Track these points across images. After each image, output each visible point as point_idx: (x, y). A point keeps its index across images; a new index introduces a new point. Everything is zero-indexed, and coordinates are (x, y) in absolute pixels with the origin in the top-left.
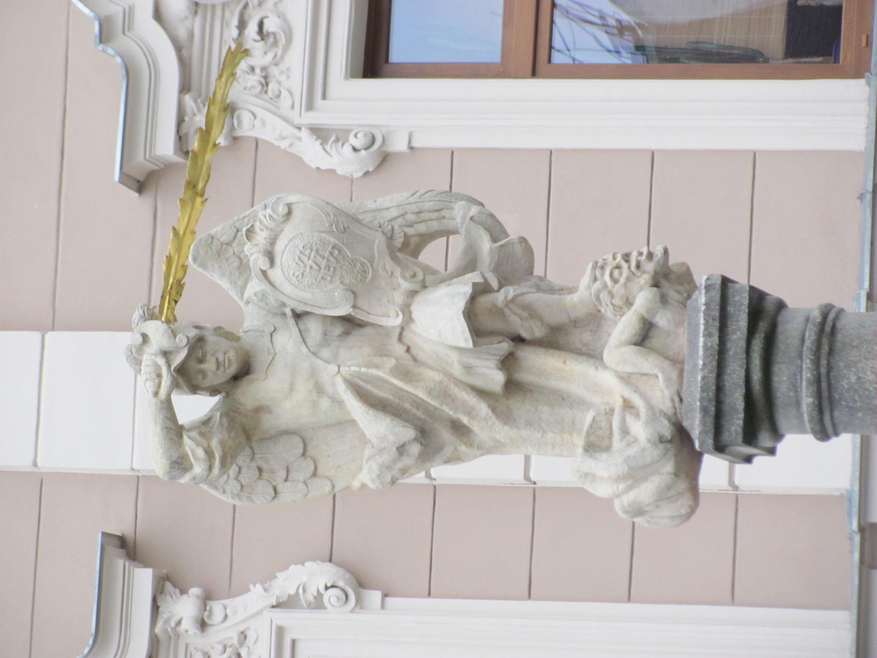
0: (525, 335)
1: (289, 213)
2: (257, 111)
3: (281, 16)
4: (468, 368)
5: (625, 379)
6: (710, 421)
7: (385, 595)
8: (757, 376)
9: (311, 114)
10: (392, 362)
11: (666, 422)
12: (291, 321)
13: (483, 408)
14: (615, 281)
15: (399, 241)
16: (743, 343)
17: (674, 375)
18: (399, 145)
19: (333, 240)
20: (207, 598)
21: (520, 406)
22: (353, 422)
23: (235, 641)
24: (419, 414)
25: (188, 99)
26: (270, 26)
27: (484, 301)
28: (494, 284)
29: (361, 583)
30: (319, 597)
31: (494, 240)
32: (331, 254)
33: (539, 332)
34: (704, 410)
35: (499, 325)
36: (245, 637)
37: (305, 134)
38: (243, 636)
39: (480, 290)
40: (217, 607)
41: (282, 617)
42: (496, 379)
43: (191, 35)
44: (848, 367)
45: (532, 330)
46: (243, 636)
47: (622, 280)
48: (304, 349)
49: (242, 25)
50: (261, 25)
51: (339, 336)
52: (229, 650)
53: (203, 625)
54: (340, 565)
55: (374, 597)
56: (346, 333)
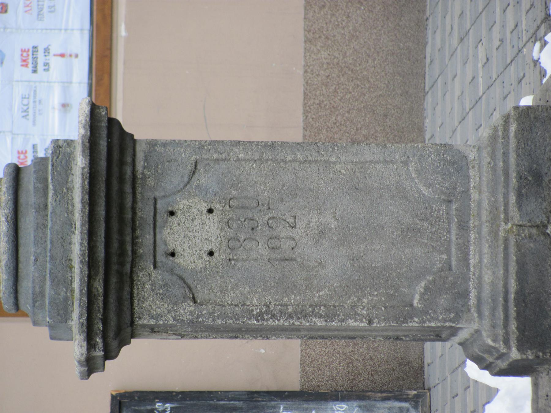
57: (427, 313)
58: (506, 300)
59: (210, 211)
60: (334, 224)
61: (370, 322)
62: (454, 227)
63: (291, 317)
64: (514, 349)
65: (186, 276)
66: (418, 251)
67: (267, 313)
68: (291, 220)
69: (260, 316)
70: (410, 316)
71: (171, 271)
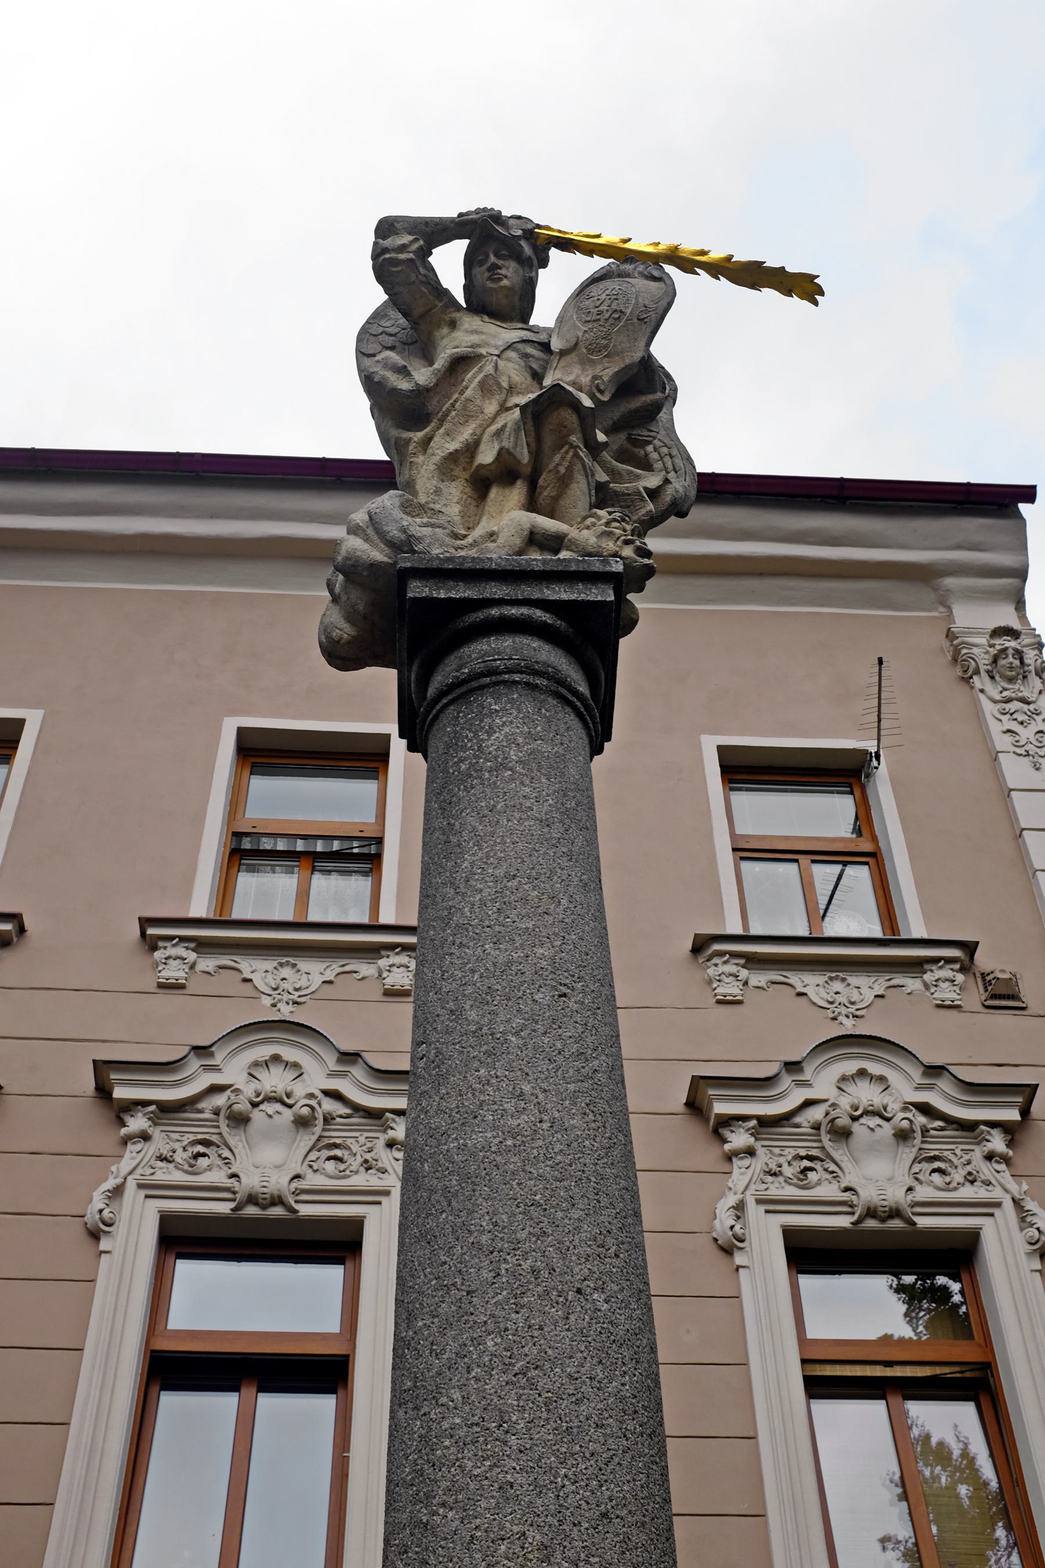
2: (750, 1171)
3: (819, 1183)
9: (754, 1202)
18: (739, 1259)
19: (628, 311)
23: (380, 1165)
25: (754, 1122)
26: (811, 1175)
32: (615, 311)
35: (548, 440)
36: (383, 1173)
37: (739, 1196)
38: (384, 1171)
43: (798, 1126)
45: (548, 486)
46: (384, 1171)
51: (531, 368)
52: (374, 1162)
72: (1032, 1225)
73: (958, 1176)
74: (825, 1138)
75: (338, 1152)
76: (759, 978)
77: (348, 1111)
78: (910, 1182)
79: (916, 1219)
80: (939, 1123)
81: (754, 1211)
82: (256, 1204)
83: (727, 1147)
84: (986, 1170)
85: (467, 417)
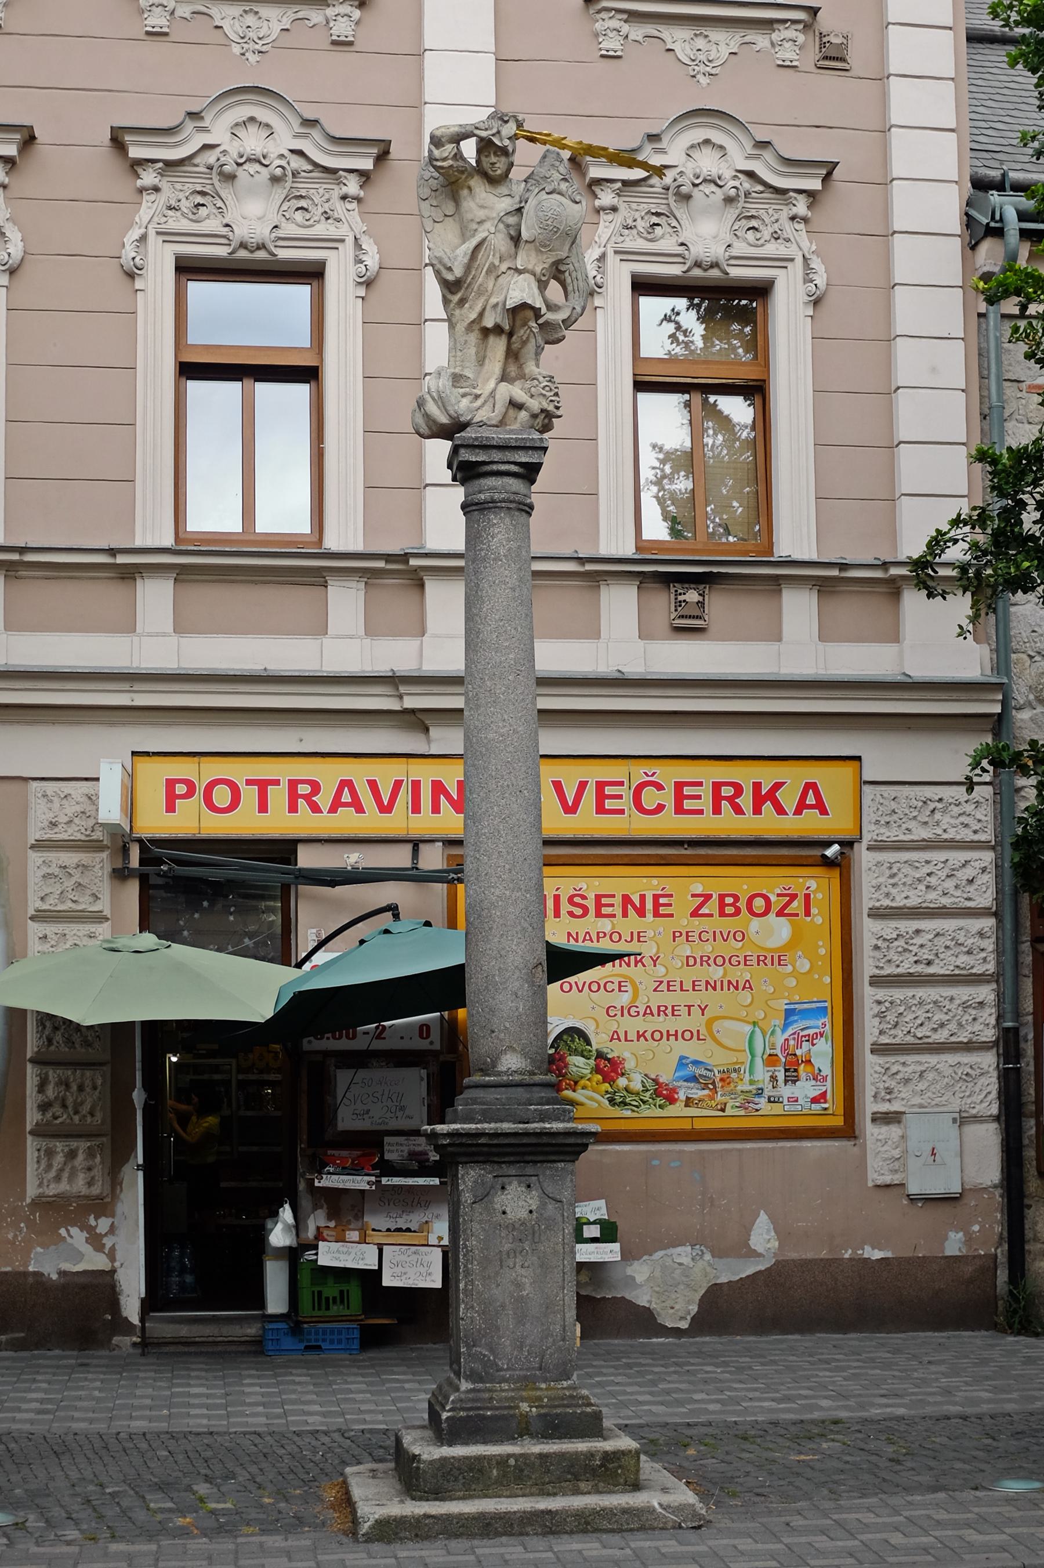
0: (514, 338)
1: (577, 203)
2: (612, 225)
4: (495, 306)
5: (492, 394)
6: (471, 442)
7: (363, 298)
8: (495, 467)
10: (497, 263)
11: (469, 418)
12: (518, 206)
13: (473, 316)
14: (543, 388)
15: (562, 268)
16: (512, 460)
17: (494, 422)
20: (359, 200)
21: (474, 337)
22: (464, 242)
23: (336, 216)
24: (469, 279)
25: (619, 185)
27: (530, 314)
28: (540, 321)
29: (369, 284)
30: (361, 261)
31: (563, 321)
33: (515, 346)
34: (476, 439)
35: (518, 323)
39: (537, 313)
40: (354, 205)
41: (350, 241)
42: (489, 322)
43: (652, 186)
44: (501, 518)
46: (339, 220)
47: (544, 392)
48: (502, 214)
49: (657, 214)
50: (658, 225)
53: (344, 198)
54: (378, 273)
55: (362, 292)
56: (512, 238)
57: (469, 1356)
58: (479, 1408)
59: (531, 1212)
60: (525, 1293)
61: (462, 1319)
62: (524, 1373)
63: (465, 1266)
64: (449, 1414)
65: (490, 1197)
66: (509, 1349)
67: (467, 1251)
68: (526, 1264)
69: (466, 1246)
70: (467, 1345)
71: (492, 1187)
72: (812, 281)
73: (766, 233)
74: (672, 200)
75: (303, 203)
76: (637, 31)
77: (310, 167)
78: (729, 238)
79: (729, 270)
80: (760, 188)
81: (612, 259)
82: (246, 248)
83: (597, 203)
84: (789, 229)
85: (480, 294)
